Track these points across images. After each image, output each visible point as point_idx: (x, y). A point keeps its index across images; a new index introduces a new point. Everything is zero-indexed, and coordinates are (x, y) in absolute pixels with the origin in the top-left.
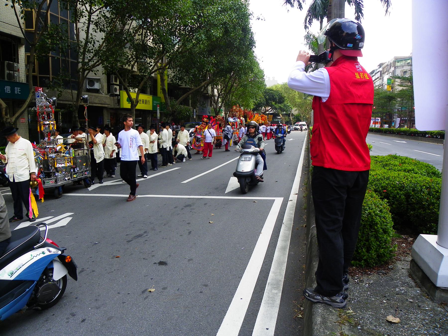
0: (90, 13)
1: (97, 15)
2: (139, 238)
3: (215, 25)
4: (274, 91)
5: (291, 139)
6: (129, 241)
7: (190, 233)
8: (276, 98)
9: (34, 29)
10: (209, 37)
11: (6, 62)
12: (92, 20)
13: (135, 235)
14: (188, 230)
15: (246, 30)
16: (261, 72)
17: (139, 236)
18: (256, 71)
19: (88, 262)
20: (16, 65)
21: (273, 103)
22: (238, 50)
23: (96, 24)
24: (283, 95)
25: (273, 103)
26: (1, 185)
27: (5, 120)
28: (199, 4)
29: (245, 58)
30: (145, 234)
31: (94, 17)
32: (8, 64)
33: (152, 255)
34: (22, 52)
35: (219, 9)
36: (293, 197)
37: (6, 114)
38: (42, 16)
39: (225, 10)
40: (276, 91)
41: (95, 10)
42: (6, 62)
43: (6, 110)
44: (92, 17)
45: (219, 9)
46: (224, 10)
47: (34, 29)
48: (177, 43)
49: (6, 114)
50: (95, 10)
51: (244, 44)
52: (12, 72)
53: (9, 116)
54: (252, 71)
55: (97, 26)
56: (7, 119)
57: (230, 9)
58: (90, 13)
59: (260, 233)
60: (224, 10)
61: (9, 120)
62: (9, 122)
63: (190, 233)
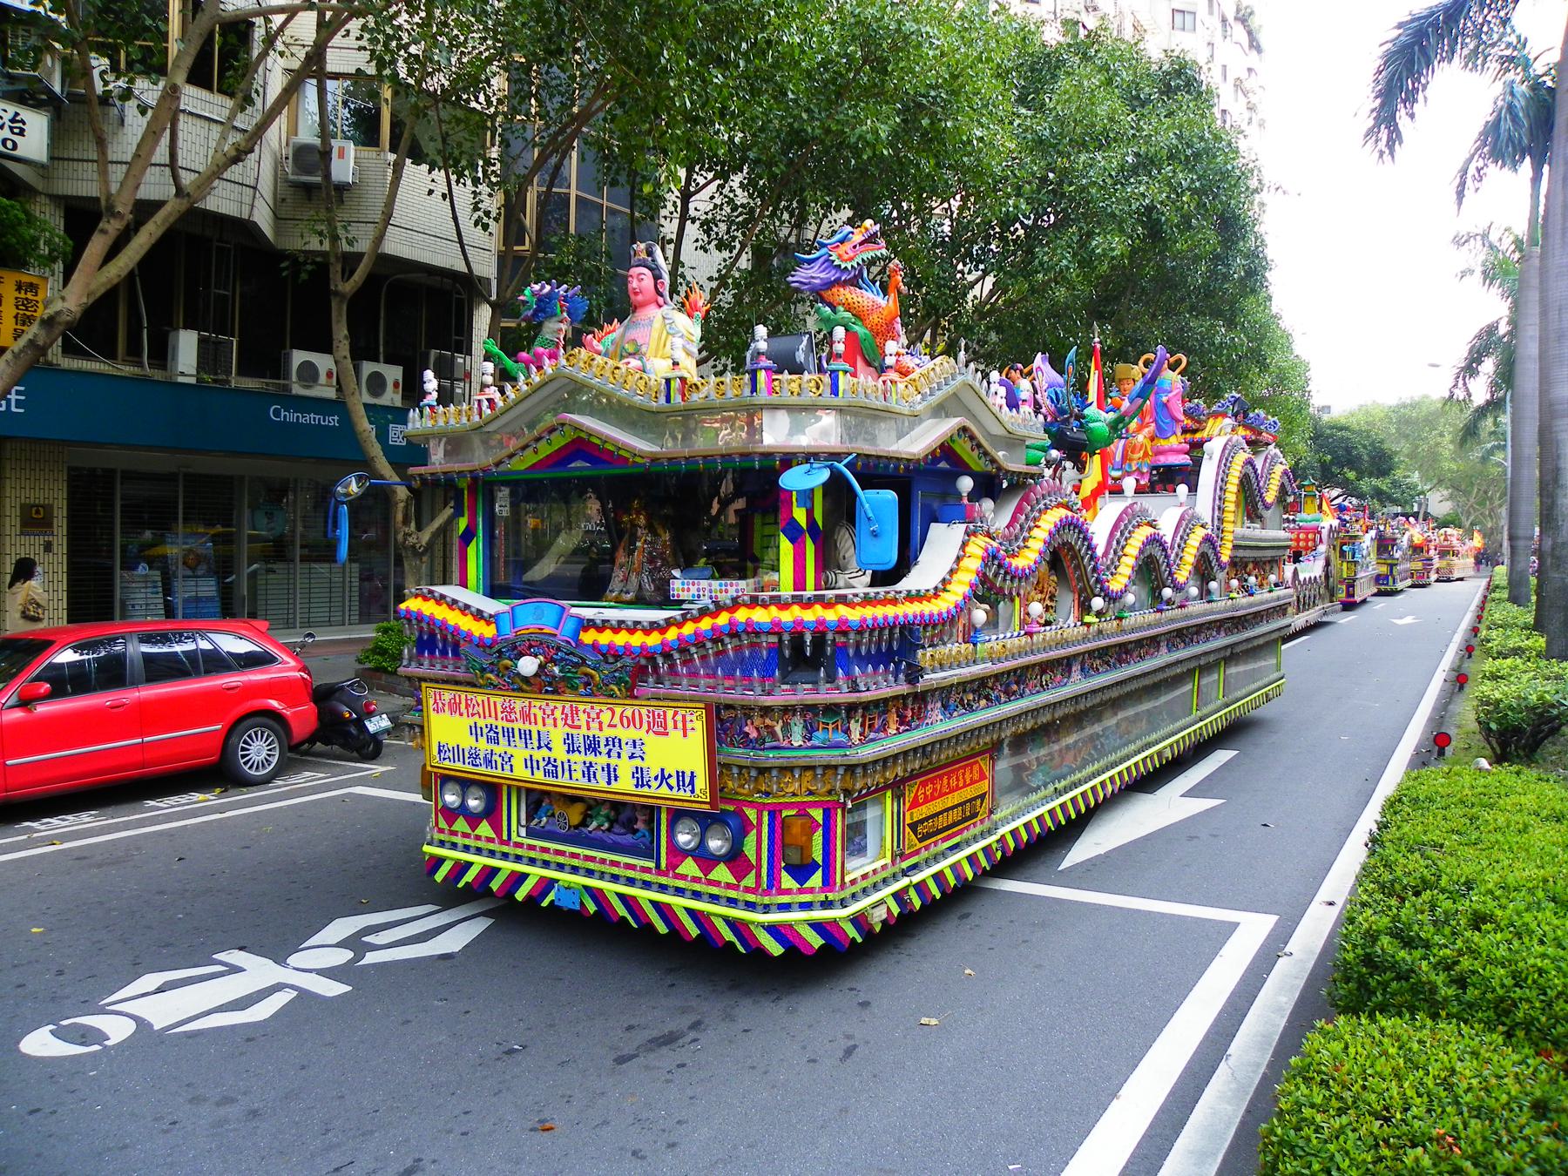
0: (686, 196)
1: (712, 198)
2: (664, 1050)
3: (1113, 215)
4: (1354, 432)
5: (1409, 620)
6: (621, 1060)
7: (849, 1052)
8: (1359, 457)
9: (527, 247)
10: (1086, 261)
11: (434, 353)
12: (692, 213)
13: (655, 1033)
14: (849, 1037)
15: (1232, 226)
16: (1301, 367)
17: (665, 1044)
18: (1276, 360)
19: (450, 1131)
20: (460, 361)
21: (1351, 475)
22: (1209, 294)
23: (707, 226)
24: (1385, 446)
25: (1351, 475)
26: (355, 754)
27: (400, 537)
28: (1054, 146)
29: (1231, 324)
30: (692, 1035)
31: (700, 204)
32: (440, 358)
33: (673, 1139)
34: (483, 317)
35: (1130, 159)
36: (1315, 928)
37: (406, 522)
38: (553, 206)
39: (1152, 162)
40: (1360, 433)
41: (701, 181)
42: (434, 353)
43: (406, 508)
44: (691, 206)
45: (1130, 159)
46: (1145, 164)
47: (527, 247)
48: (977, 281)
49: (406, 522)
50: (701, 181)
51: (1226, 277)
52: (447, 383)
53: (413, 524)
54: (1264, 367)
55: (708, 232)
56: (406, 534)
57: (1171, 157)
58: (686, 196)
59: (1114, 1095)
60: (1145, 164)
61: (412, 540)
62: (413, 547)
63: (849, 1052)
